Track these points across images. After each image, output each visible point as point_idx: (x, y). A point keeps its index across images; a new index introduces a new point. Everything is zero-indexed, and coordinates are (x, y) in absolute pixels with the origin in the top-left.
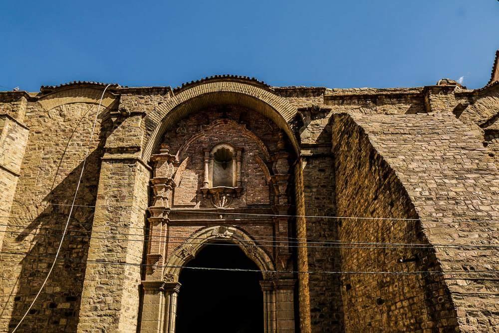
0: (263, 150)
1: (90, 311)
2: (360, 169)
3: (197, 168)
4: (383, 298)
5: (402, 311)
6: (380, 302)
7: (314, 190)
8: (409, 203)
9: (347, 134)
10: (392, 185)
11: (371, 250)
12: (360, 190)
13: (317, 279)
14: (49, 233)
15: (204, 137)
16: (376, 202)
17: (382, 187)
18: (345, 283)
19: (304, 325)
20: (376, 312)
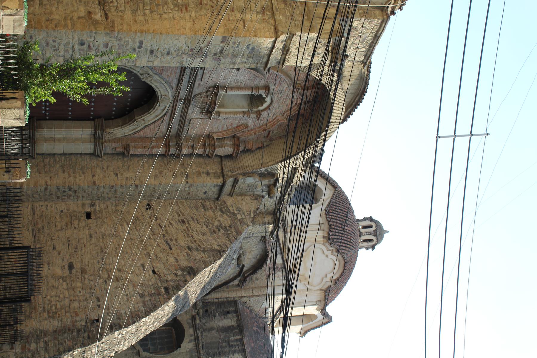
0: (252, 130)
1: (79, 39)
2: (187, 250)
4: (74, 271)
5: (62, 296)
6: (71, 267)
7: (187, 189)
8: (137, 318)
9: (230, 226)
10: (157, 296)
12: (168, 247)
13: (98, 189)
15: (287, 86)
16: (151, 273)
17: (160, 285)
19: (58, 166)
20: (63, 260)
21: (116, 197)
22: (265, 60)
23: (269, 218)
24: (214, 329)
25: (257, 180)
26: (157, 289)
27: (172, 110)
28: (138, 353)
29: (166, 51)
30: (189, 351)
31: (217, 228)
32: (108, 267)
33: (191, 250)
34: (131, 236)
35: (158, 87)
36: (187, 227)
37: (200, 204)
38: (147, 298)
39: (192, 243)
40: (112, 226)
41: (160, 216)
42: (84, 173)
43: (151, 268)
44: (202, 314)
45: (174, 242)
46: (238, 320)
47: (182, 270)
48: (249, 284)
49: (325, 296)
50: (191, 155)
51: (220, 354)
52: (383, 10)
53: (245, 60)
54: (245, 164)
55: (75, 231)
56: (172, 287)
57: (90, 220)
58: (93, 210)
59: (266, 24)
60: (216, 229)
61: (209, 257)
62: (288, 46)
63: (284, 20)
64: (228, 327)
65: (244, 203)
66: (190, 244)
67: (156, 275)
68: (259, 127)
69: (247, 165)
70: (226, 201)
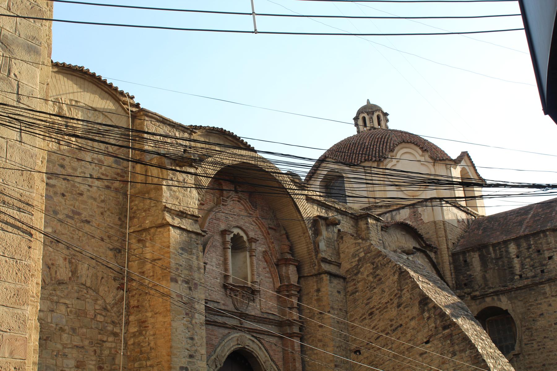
0: (269, 247)
2: (401, 308)
3: (218, 253)
7: (336, 312)
8: (479, 358)
9: (373, 264)
10: (454, 337)
12: (399, 329)
14: (71, 311)
16: (429, 345)
17: (441, 335)
22: (193, 236)
23: (362, 224)
24: (485, 276)
25: (321, 238)
26: (445, 338)
27: (253, 332)
28: (517, 355)
29: (189, 341)
30: (510, 301)
31: (375, 277)
33: (401, 304)
35: (228, 348)
36: (377, 309)
37: (351, 297)
38: (456, 347)
39: (393, 303)
41: (367, 339)
43: (423, 346)
44: (469, 290)
45: (393, 322)
46: (473, 250)
47: (423, 311)
48: (434, 241)
49: (440, 160)
50: (300, 309)
51: (511, 268)
52: (134, 116)
53: (195, 257)
54: (306, 252)
56: (442, 321)
59: (155, 237)
60: (377, 278)
61: (407, 283)
62: (178, 213)
63: (151, 218)
64: (480, 261)
65: (347, 250)
66: (394, 305)
67: (431, 340)
68: (266, 239)
69: (306, 249)
70: (346, 270)
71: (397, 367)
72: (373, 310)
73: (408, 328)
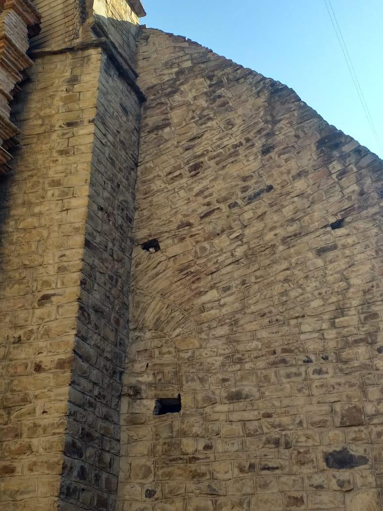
2: (272, 154)
4: (357, 450)
6: (341, 460)
9: (210, 78)
11: (305, 328)
12: (265, 195)
13: (86, 359)
18: (146, 392)
20: (320, 487)
21: (117, 322)
31: (214, 100)
32: (332, 345)
33: (273, 148)
34: (233, 284)
37: (153, 135)
39: (253, 145)
40: (203, 336)
42: (25, 400)
43: (325, 233)
47: (329, 160)
54: (59, 13)
55: (219, 446)
57: (183, 401)
58: (152, 393)
66: (255, 150)
69: (61, 6)
70: (146, 86)
71: (253, 280)
72: (201, 160)
73: (288, 194)
